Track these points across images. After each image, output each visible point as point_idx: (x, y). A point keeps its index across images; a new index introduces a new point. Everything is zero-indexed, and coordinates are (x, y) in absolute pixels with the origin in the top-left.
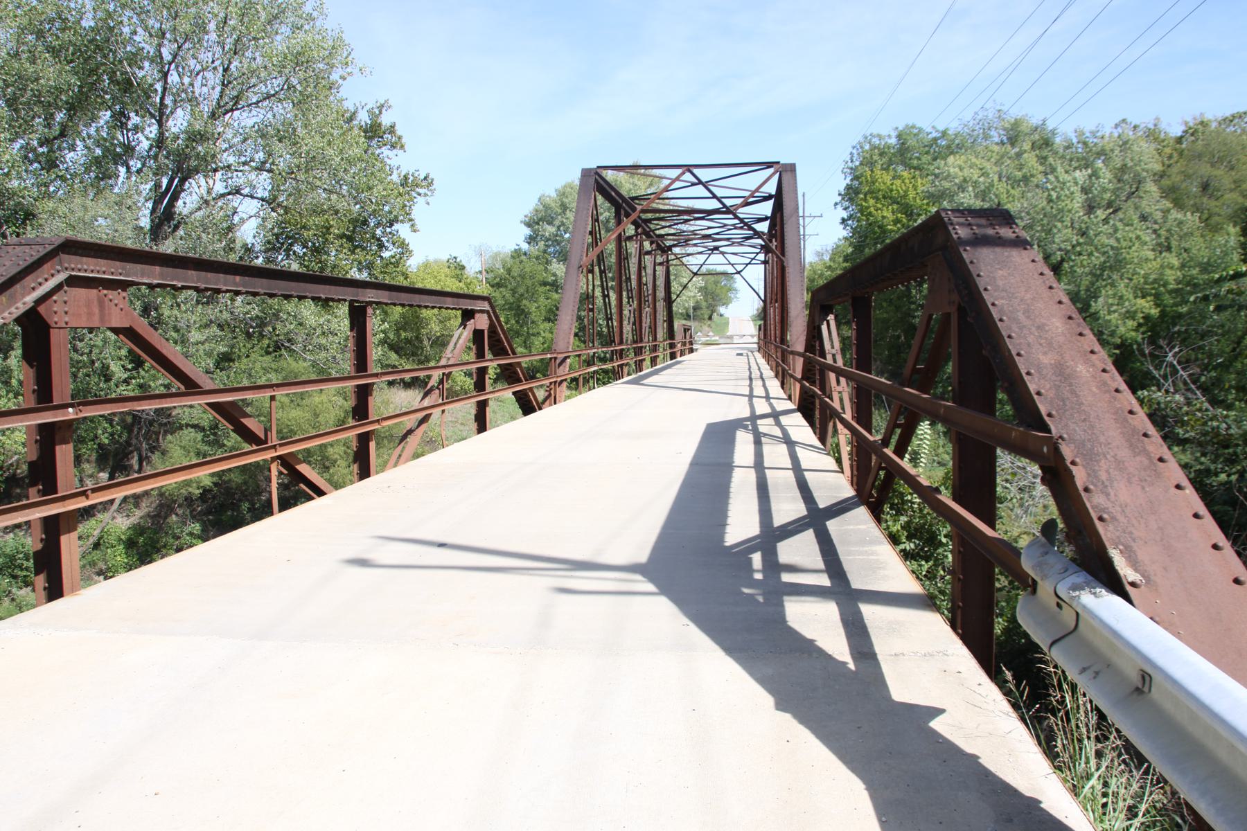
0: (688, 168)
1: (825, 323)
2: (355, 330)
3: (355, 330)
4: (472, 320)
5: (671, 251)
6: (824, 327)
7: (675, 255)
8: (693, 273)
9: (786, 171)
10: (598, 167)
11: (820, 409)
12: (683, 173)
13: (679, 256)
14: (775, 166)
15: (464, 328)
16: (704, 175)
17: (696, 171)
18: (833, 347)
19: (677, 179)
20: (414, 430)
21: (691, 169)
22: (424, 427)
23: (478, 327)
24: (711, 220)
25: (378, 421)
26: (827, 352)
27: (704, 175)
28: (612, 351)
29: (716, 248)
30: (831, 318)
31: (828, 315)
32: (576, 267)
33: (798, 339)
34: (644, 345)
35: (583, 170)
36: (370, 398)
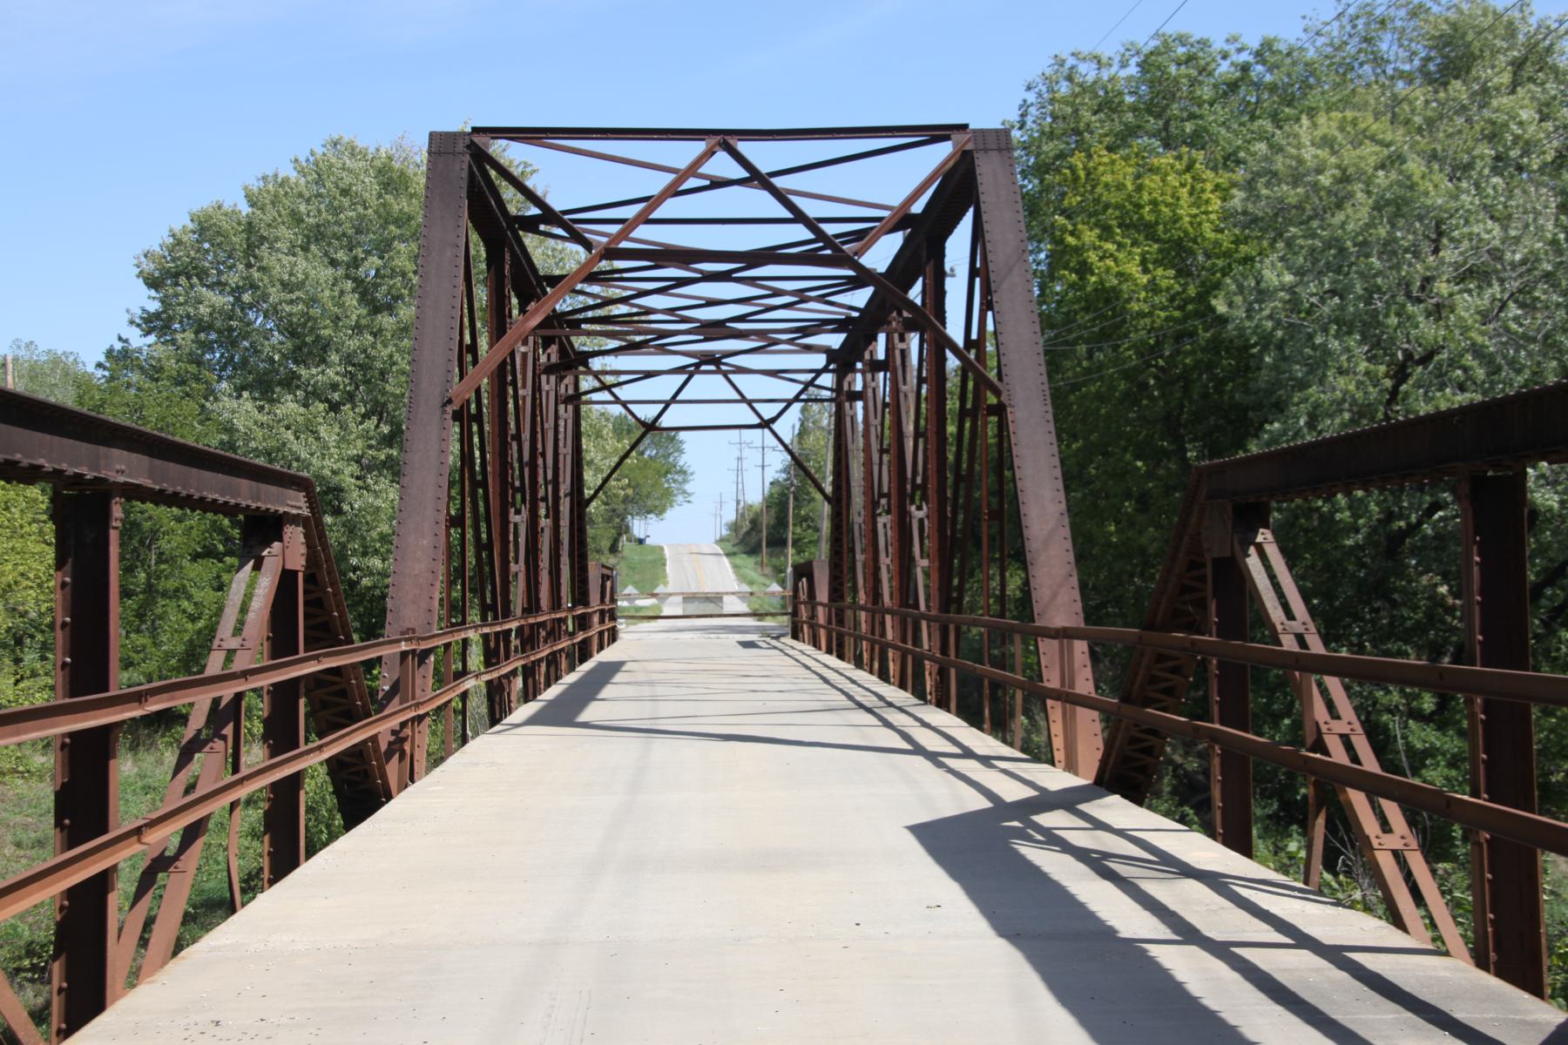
0: (725, 140)
1: (1252, 550)
2: (68, 567)
3: (68, 567)
4: (276, 545)
5: (586, 365)
6: (1253, 562)
7: (596, 375)
8: (643, 423)
9: (986, 150)
10: (476, 130)
11: (1223, 783)
12: (709, 153)
13: (609, 379)
14: (956, 136)
15: (257, 567)
16: (764, 156)
17: (743, 147)
18: (1290, 615)
19: (692, 170)
20: (176, 857)
21: (732, 141)
22: (198, 846)
23: (289, 567)
24: (751, 281)
25: (138, 832)
26: (1279, 628)
27: (764, 156)
28: (497, 634)
29: (714, 360)
30: (1264, 536)
31: (1256, 533)
32: (436, 402)
33: (1054, 595)
34: (562, 615)
35: (432, 135)
36: (112, 762)
